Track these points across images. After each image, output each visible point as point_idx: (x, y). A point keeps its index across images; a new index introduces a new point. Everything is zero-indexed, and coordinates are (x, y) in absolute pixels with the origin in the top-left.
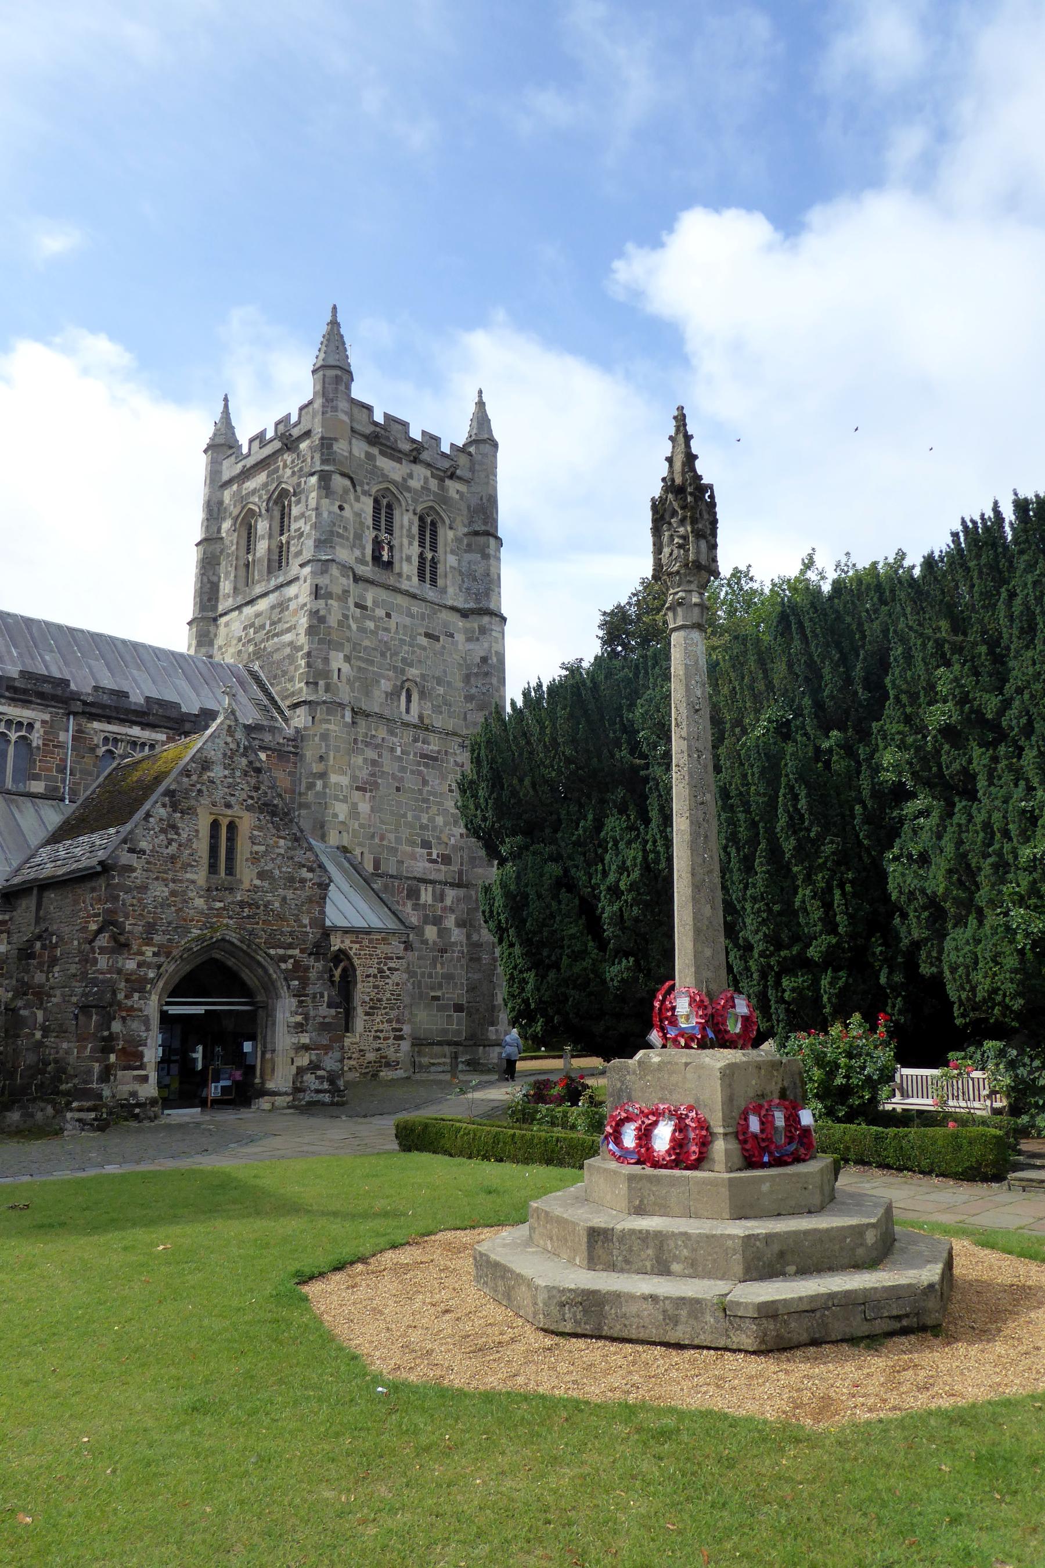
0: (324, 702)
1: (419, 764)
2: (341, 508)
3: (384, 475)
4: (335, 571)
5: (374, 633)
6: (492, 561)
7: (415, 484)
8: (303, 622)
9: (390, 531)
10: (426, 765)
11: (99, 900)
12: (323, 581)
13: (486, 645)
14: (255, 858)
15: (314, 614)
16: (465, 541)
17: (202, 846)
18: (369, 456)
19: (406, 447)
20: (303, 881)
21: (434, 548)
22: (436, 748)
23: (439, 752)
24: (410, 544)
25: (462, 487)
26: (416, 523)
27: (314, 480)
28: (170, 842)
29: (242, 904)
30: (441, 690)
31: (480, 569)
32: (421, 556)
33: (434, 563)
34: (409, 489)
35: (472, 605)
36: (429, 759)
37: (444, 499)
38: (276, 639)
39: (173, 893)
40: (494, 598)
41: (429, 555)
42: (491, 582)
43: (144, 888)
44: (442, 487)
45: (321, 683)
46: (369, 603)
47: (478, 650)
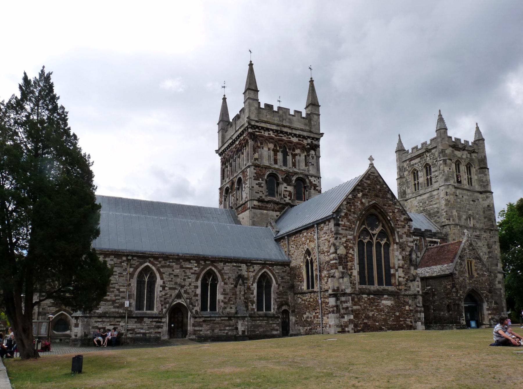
0: (453, 224)
1: (475, 239)
2: (450, 169)
3: (457, 156)
4: (451, 187)
5: (460, 202)
6: (487, 176)
7: (464, 157)
8: (443, 202)
9: (459, 172)
10: (477, 239)
11: (450, 281)
12: (448, 191)
13: (489, 201)
14: (476, 270)
15: (447, 200)
16: (479, 171)
17: (466, 268)
18: (453, 151)
19: (460, 146)
20: (485, 275)
21: (470, 175)
22: (478, 233)
23: (479, 234)
24: (465, 175)
25: (476, 155)
26: (466, 168)
27: (441, 162)
28: (461, 267)
29: (475, 281)
30: (477, 216)
31: (484, 179)
32: (468, 178)
33: (471, 179)
34: (463, 159)
35: (483, 190)
36: (478, 237)
37: (471, 159)
38: (431, 206)
39: (464, 279)
40: (489, 186)
41: (469, 177)
42: (488, 182)
43: (458, 278)
44: (471, 156)
45: (451, 219)
46: (458, 194)
47: (486, 203)
